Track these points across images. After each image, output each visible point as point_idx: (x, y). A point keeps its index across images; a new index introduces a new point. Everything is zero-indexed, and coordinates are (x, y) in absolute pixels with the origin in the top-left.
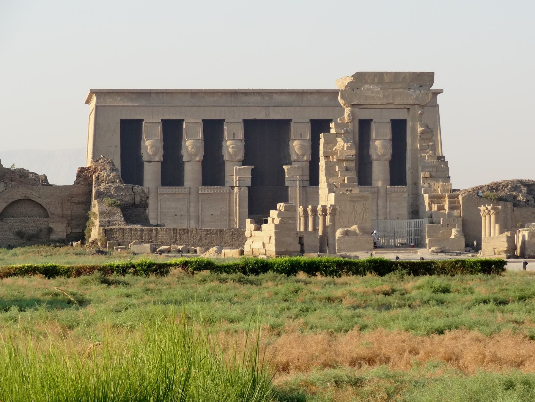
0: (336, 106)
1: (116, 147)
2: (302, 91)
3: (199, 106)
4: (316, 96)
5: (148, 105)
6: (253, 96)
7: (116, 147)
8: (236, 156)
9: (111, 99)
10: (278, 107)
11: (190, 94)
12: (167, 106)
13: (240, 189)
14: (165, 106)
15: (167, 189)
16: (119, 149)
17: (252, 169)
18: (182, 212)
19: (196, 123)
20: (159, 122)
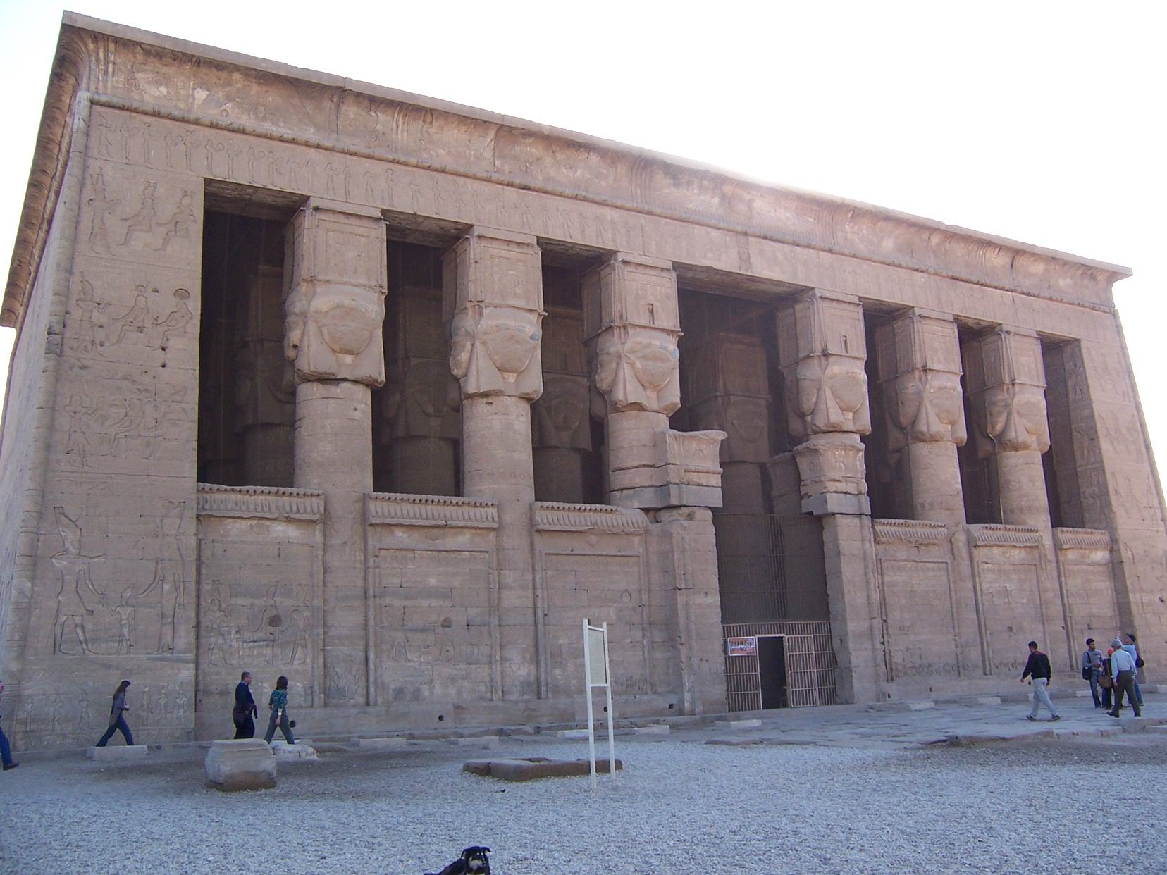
0: (917, 270)
1: (182, 293)
2: (840, 201)
3: (526, 188)
4: (865, 228)
5: (327, 144)
6: (696, 191)
7: (182, 293)
8: (659, 391)
9: (163, 90)
10: (770, 242)
11: (492, 134)
12: (406, 164)
13: (690, 517)
14: (393, 161)
15: (410, 507)
16: (195, 305)
17: (725, 447)
18: (473, 612)
19: (518, 244)
20: (377, 219)
